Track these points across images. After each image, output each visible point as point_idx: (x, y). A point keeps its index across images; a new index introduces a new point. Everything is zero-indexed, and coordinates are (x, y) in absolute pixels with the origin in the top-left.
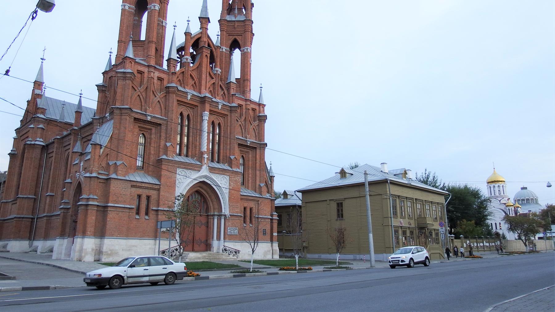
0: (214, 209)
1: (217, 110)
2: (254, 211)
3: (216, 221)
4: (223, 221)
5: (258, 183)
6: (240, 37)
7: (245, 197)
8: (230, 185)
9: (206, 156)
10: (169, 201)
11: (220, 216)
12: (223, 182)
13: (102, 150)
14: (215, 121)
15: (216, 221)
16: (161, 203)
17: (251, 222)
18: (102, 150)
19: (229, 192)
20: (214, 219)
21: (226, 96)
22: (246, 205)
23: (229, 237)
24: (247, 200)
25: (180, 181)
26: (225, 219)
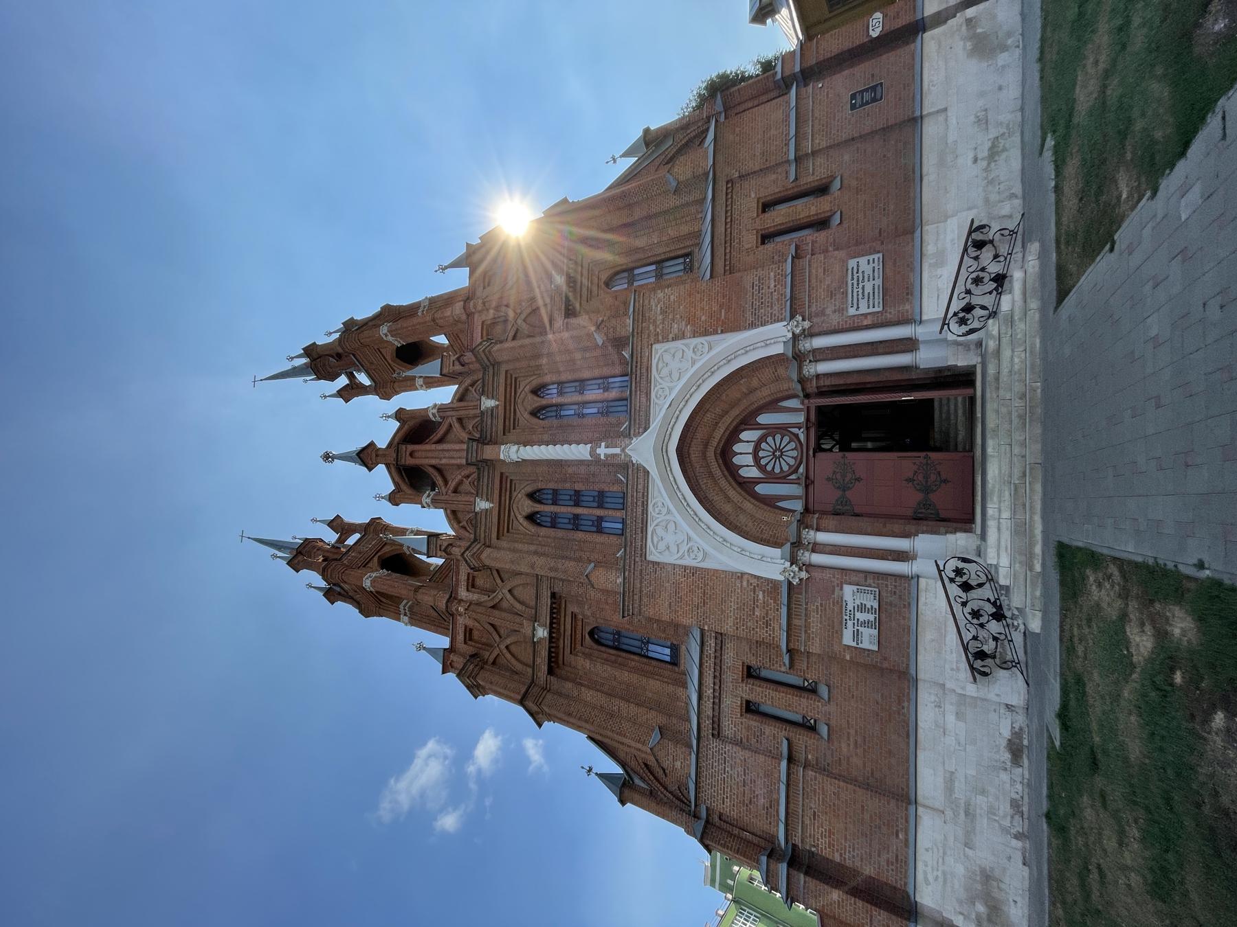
0: (778, 379)
2: (771, 185)
4: (820, 342)
5: (673, 201)
7: (720, 251)
9: (602, 451)
10: (755, 600)
11: (799, 358)
13: (637, 781)
14: (530, 408)
16: (763, 634)
17: (822, 190)
18: (637, 781)
20: (818, 376)
22: (750, 239)
23: (900, 292)
24: (729, 240)
25: (684, 548)
26: (812, 335)
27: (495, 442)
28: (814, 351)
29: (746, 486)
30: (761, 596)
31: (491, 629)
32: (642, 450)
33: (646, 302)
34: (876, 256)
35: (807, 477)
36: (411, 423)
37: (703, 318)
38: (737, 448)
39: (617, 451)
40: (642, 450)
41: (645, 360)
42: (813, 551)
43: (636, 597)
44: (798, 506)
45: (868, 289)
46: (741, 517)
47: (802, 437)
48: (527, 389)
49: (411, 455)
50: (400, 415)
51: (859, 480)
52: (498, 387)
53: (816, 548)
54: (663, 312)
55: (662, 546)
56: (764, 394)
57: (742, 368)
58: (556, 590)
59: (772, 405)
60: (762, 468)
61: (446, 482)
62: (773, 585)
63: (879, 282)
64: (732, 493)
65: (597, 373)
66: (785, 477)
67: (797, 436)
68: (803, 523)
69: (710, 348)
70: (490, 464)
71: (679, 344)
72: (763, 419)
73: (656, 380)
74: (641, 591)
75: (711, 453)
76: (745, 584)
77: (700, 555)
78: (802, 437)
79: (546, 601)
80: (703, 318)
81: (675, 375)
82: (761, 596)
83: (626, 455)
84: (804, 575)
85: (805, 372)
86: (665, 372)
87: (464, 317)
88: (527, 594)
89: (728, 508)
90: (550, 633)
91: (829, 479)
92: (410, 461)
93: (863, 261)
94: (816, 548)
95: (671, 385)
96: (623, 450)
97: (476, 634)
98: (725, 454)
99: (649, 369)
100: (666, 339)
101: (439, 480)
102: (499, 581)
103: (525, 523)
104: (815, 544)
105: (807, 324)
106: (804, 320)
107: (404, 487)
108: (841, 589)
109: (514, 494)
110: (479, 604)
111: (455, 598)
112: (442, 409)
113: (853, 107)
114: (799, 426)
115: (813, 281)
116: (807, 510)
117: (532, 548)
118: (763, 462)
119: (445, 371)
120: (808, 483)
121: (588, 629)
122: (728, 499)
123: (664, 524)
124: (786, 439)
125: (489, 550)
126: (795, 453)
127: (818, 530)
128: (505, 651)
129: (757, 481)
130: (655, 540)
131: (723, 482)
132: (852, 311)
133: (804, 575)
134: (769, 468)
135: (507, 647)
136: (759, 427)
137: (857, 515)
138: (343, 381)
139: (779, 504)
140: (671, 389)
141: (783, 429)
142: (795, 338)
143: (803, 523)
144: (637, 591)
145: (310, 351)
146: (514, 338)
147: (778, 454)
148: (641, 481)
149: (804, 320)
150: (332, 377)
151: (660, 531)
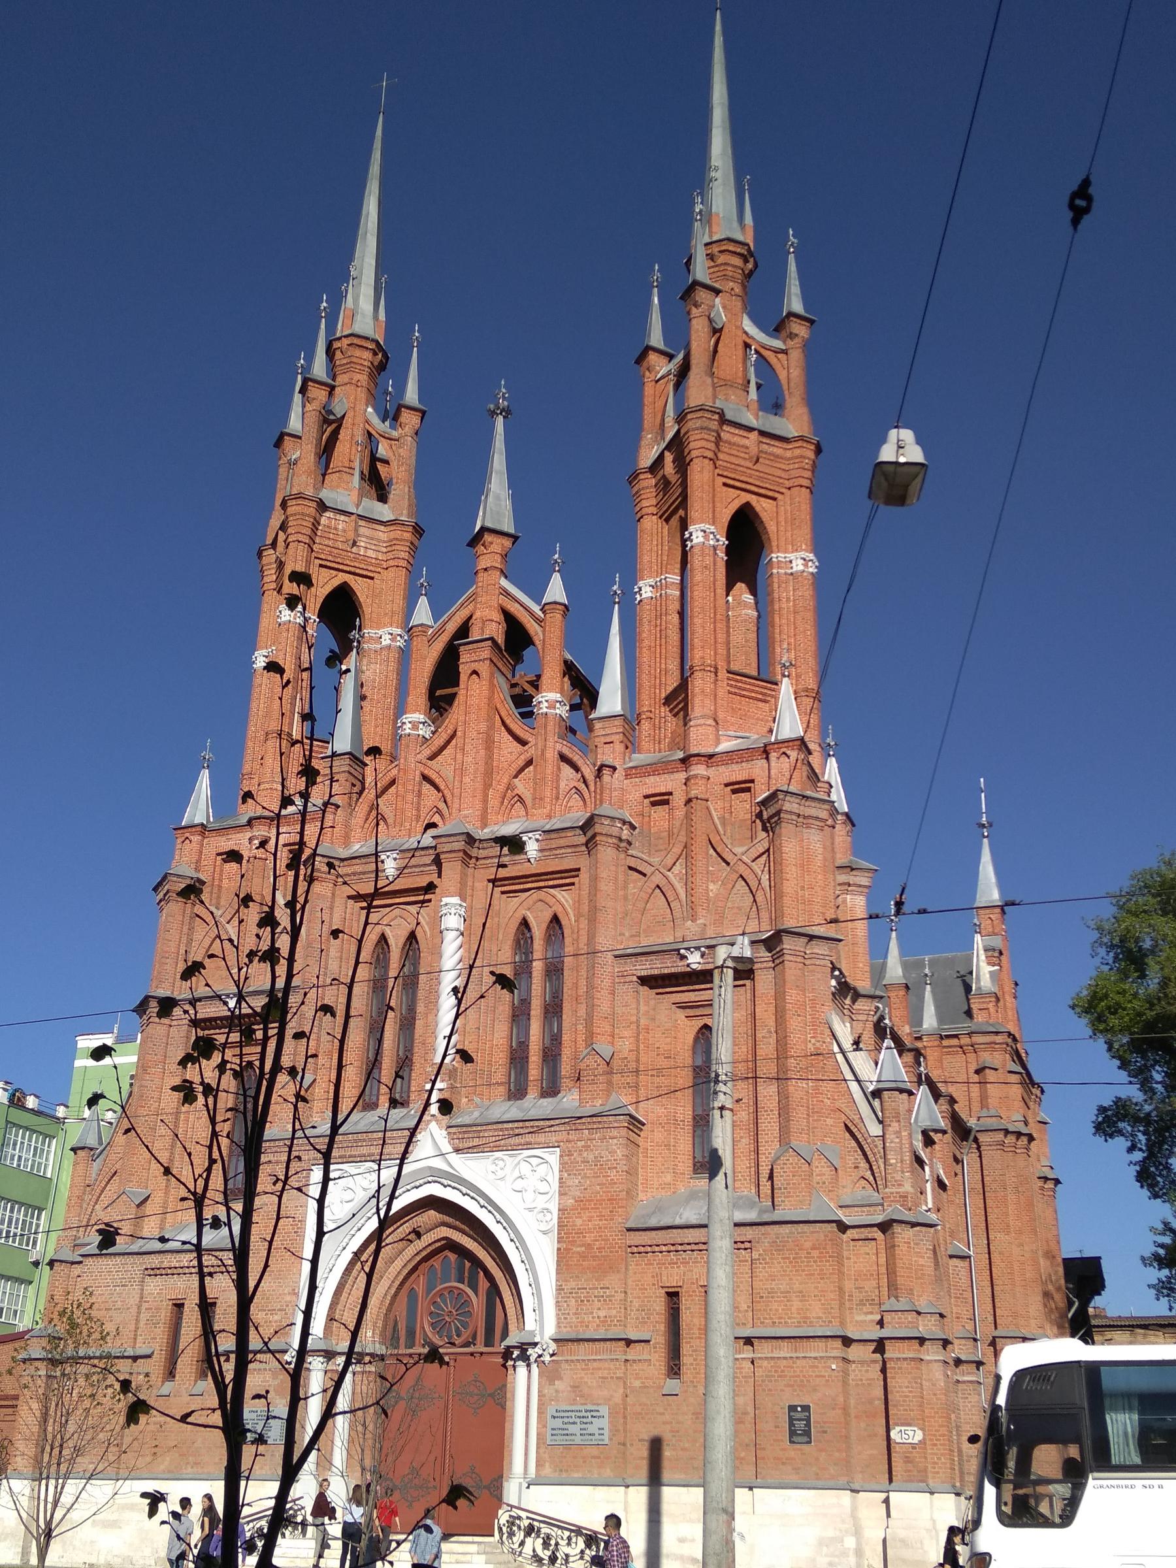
19: (561, 1226)
21: (592, 788)
34: (606, 1438)
37: (579, 1222)
45: (572, 1429)
63: (578, 1440)
80: (579, 1222)
93: (605, 1423)
99: (528, 1146)
100: (564, 1167)
113: (792, 1408)
115: (595, 1365)
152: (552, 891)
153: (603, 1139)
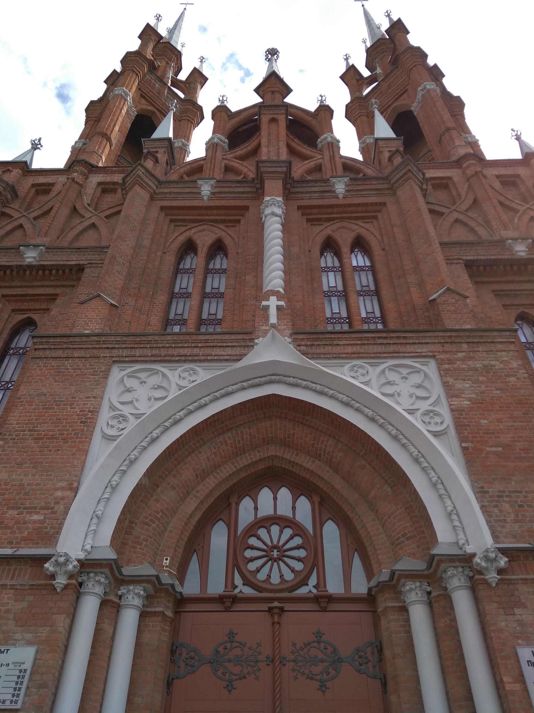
1: (334, 201)
3: (419, 615)
6: (405, 96)
8: (450, 392)
9: (273, 303)
10: (32, 510)
12: (405, 388)
15: (419, 615)
20: (404, 609)
25: (126, 410)
26: (473, 589)
27: (288, 195)
28: (448, 599)
29: (221, 508)
30: (35, 517)
31: (46, 208)
32: (274, 350)
33: (500, 346)
35: (235, 600)
36: (314, 123)
37: (484, 422)
38: (285, 494)
39: (273, 319)
40: (274, 350)
41: (409, 348)
42: (104, 603)
43: (60, 353)
44: (191, 587)
46: (172, 493)
47: (303, 591)
48: (363, 232)
49: (273, 120)
50: (325, 111)
51: (230, 687)
52: (363, 196)
53: (110, 608)
54: (487, 369)
55: (130, 383)
56: (368, 523)
57: (405, 481)
58: (87, 270)
59: (355, 543)
60: (252, 530)
61: (242, 158)
62: (51, 536)
64: (211, 482)
65: (389, 306)
66: (236, 565)
67: (304, 582)
68: (156, 589)
69: (436, 434)
70: (259, 193)
71: (437, 389)
72: (331, 531)
73: (378, 365)
74: (67, 358)
75: (272, 451)
76: (59, 494)
77: (110, 432)
78: (303, 591)
79: (74, 260)
80: (484, 422)
81: (389, 390)
82: (35, 517)
83: (266, 332)
84: (61, 581)
85: (409, 585)
86: (392, 376)
87: (454, 158)
88: (89, 240)
89: (187, 473)
90: (30, 267)
91: (231, 635)
92: (265, 119)
94: (110, 608)
95: (374, 382)
96: (273, 326)
97: (43, 198)
98: (273, 476)
100: (443, 373)
101: (241, 150)
102: (108, 213)
103: (182, 238)
104: (118, 608)
105: (492, 577)
106: (500, 571)
107: (234, 121)
108: (30, 643)
109: (222, 226)
110: (80, 194)
111: (90, 172)
112: (334, 145)
114: (321, 583)
116: (181, 602)
117: (146, 243)
118: (262, 532)
119: (381, 143)
120: (228, 601)
121: (36, 317)
122: (202, 475)
123: (164, 384)
124: (299, 566)
125: (146, 196)
126: (275, 579)
127: (143, 615)
128: (16, 223)
129: (232, 525)
130: (143, 375)
131: (227, 470)
132: (525, 654)
133: (61, 581)
134: (253, 541)
135: (21, 226)
136: (318, 523)
137: (169, 684)
138: (366, 73)
139: (195, 558)
140: (366, 383)
141: (315, 560)
142: (467, 560)
143: (156, 589)
144: (68, 353)
145: (398, 28)
146: (431, 211)
147: (275, 554)
148: (229, 351)
149: (500, 571)
150: (368, 66)
151: (155, 380)
152: (359, 222)
153: (488, 352)
